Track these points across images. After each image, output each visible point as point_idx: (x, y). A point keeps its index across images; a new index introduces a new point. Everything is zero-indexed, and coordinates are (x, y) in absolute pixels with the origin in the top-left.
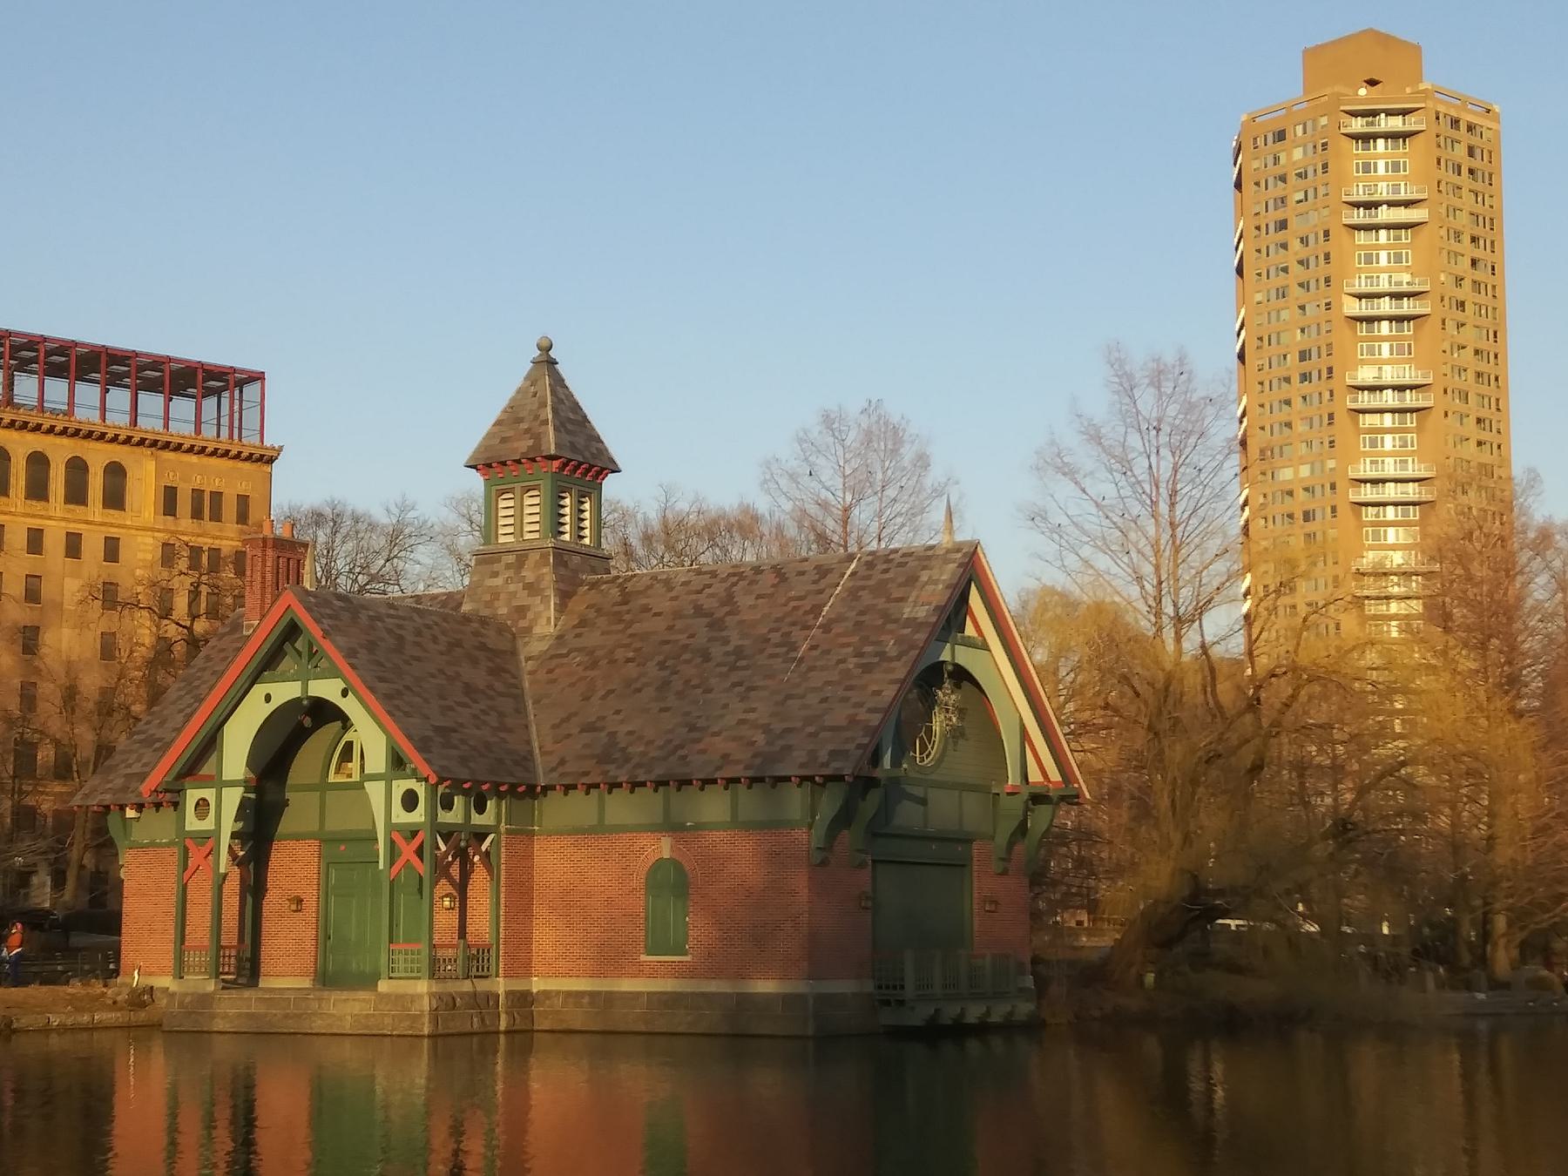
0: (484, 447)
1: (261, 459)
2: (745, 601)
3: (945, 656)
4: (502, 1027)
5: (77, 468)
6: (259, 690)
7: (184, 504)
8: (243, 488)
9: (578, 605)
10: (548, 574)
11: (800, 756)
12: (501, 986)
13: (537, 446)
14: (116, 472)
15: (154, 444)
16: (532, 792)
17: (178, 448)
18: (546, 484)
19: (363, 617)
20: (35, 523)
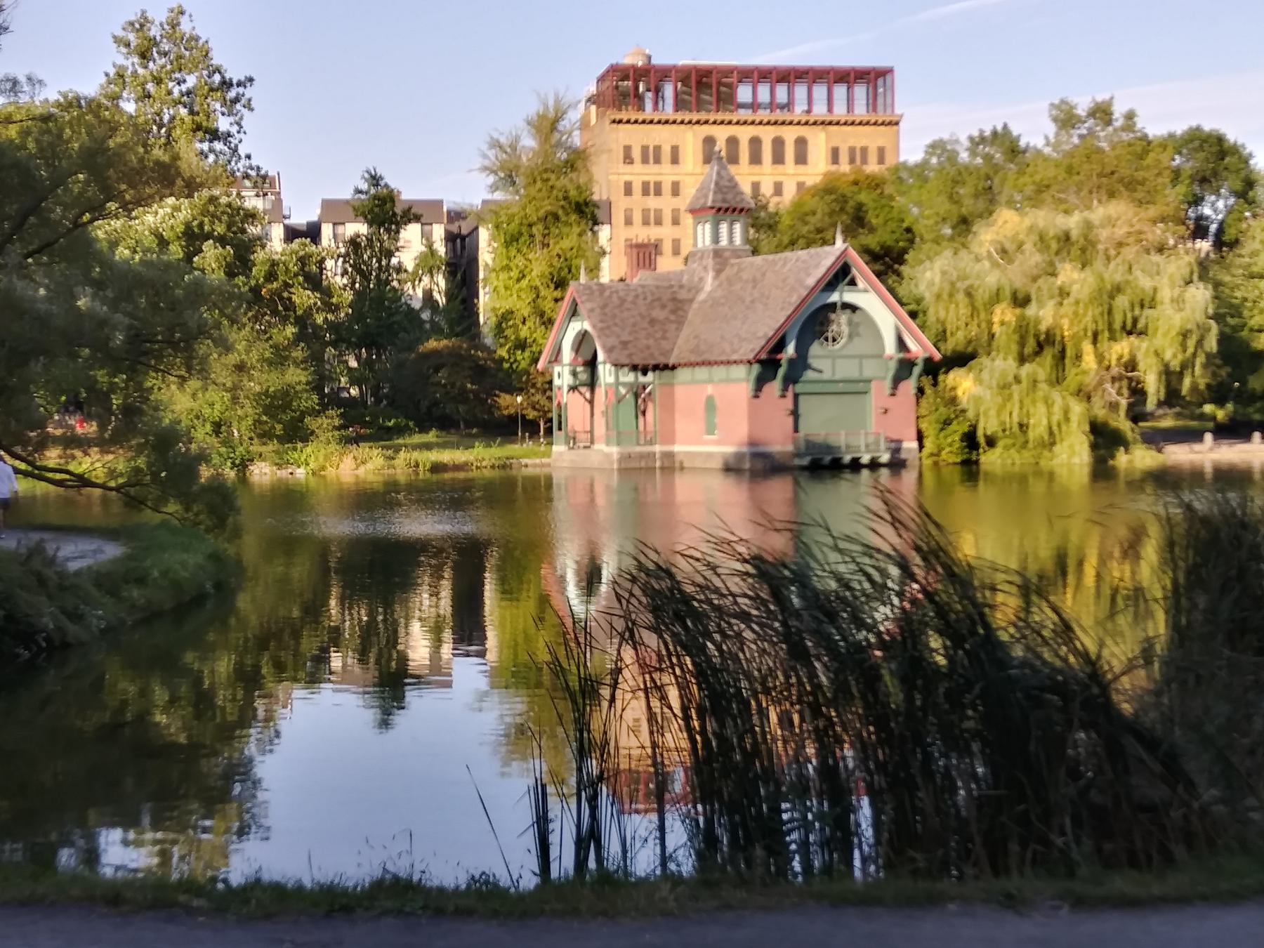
0: (691, 203)
1: (890, 123)
2: (768, 274)
3: (835, 297)
4: (658, 464)
5: (778, 143)
6: (572, 324)
7: (844, 157)
8: (881, 142)
9: (723, 276)
10: (710, 262)
11: (742, 351)
12: (657, 448)
13: (705, 203)
14: (801, 143)
15: (823, 123)
16: (666, 367)
17: (838, 123)
18: (710, 218)
19: (607, 293)
20: (756, 179)
